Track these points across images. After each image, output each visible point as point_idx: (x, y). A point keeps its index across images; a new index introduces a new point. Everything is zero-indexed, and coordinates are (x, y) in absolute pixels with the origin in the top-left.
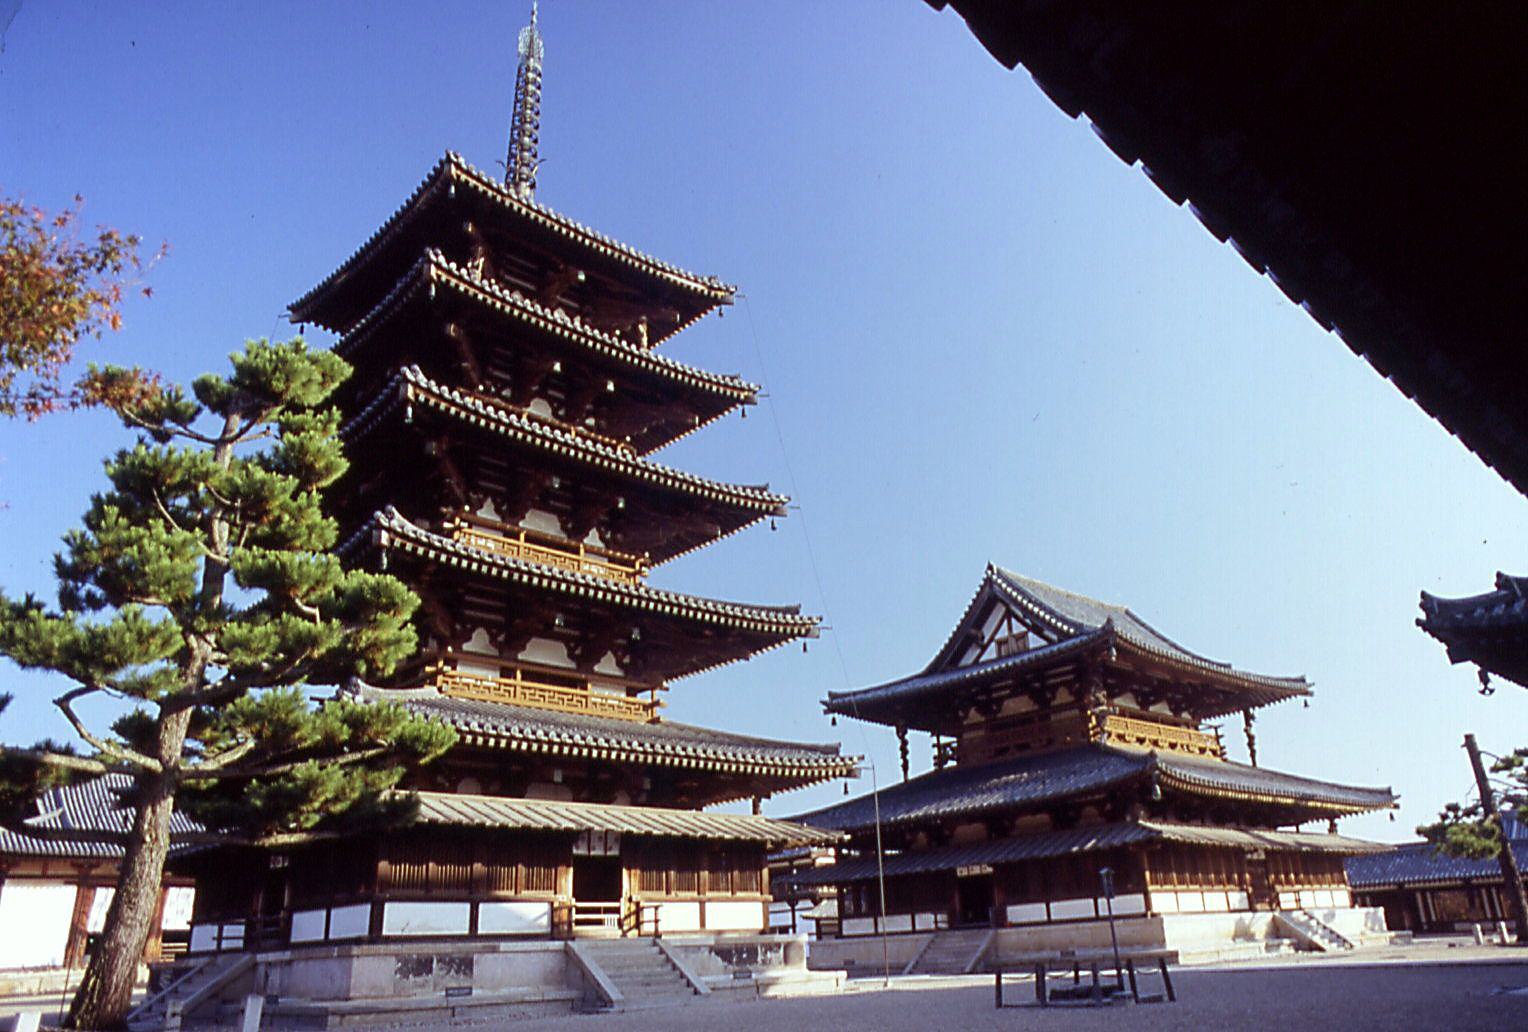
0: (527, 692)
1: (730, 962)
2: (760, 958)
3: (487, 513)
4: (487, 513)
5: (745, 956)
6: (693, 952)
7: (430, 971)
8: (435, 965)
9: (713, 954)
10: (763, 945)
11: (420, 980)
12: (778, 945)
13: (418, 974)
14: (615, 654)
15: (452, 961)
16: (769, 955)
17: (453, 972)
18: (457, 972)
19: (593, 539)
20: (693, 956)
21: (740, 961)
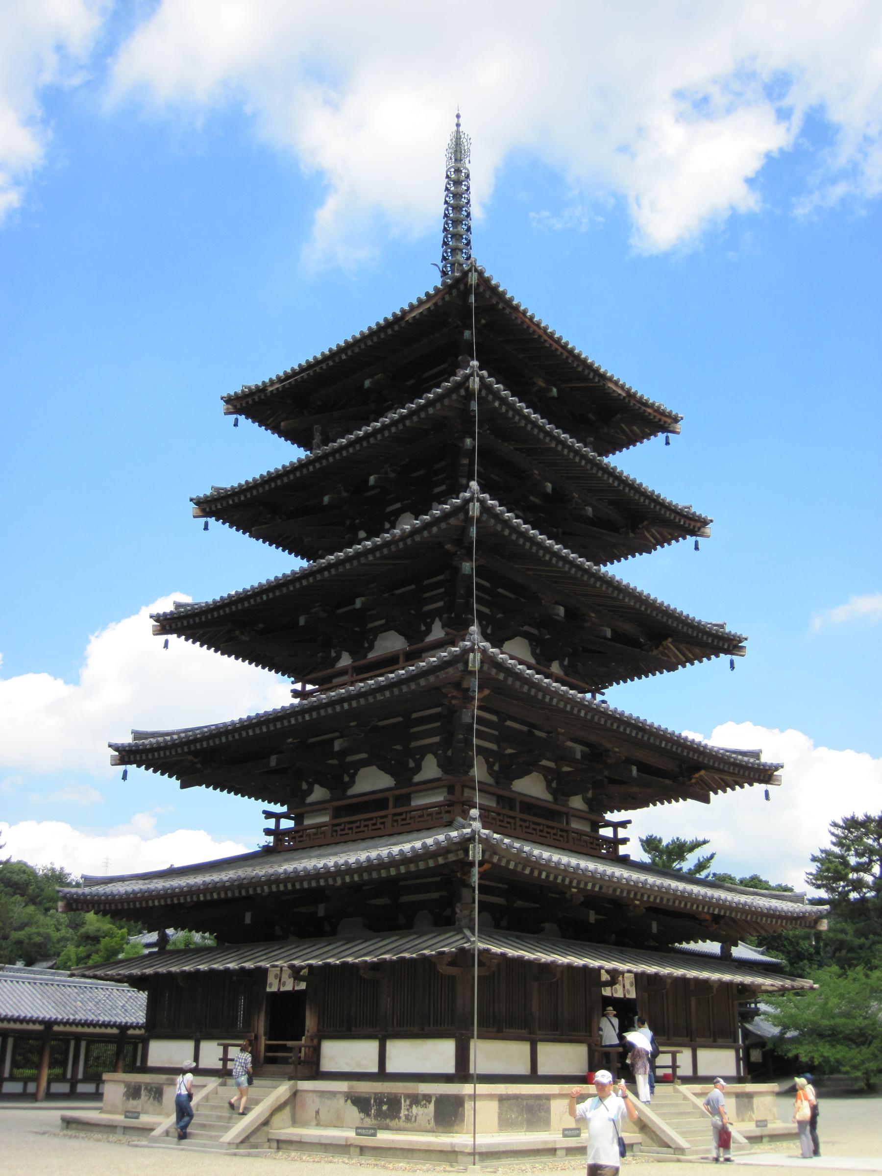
0: (338, 828)
1: (368, 1114)
2: (403, 1113)
3: (345, 661)
4: (345, 661)
5: (385, 1108)
6: (329, 1099)
7: (139, 1097)
8: (143, 1092)
9: (349, 1101)
10: (408, 1096)
11: (135, 1102)
12: (427, 1098)
13: (134, 1099)
14: (436, 755)
15: (151, 1088)
16: (415, 1110)
17: (151, 1099)
18: (154, 1098)
19: (438, 632)
20: (328, 1102)
21: (380, 1114)
